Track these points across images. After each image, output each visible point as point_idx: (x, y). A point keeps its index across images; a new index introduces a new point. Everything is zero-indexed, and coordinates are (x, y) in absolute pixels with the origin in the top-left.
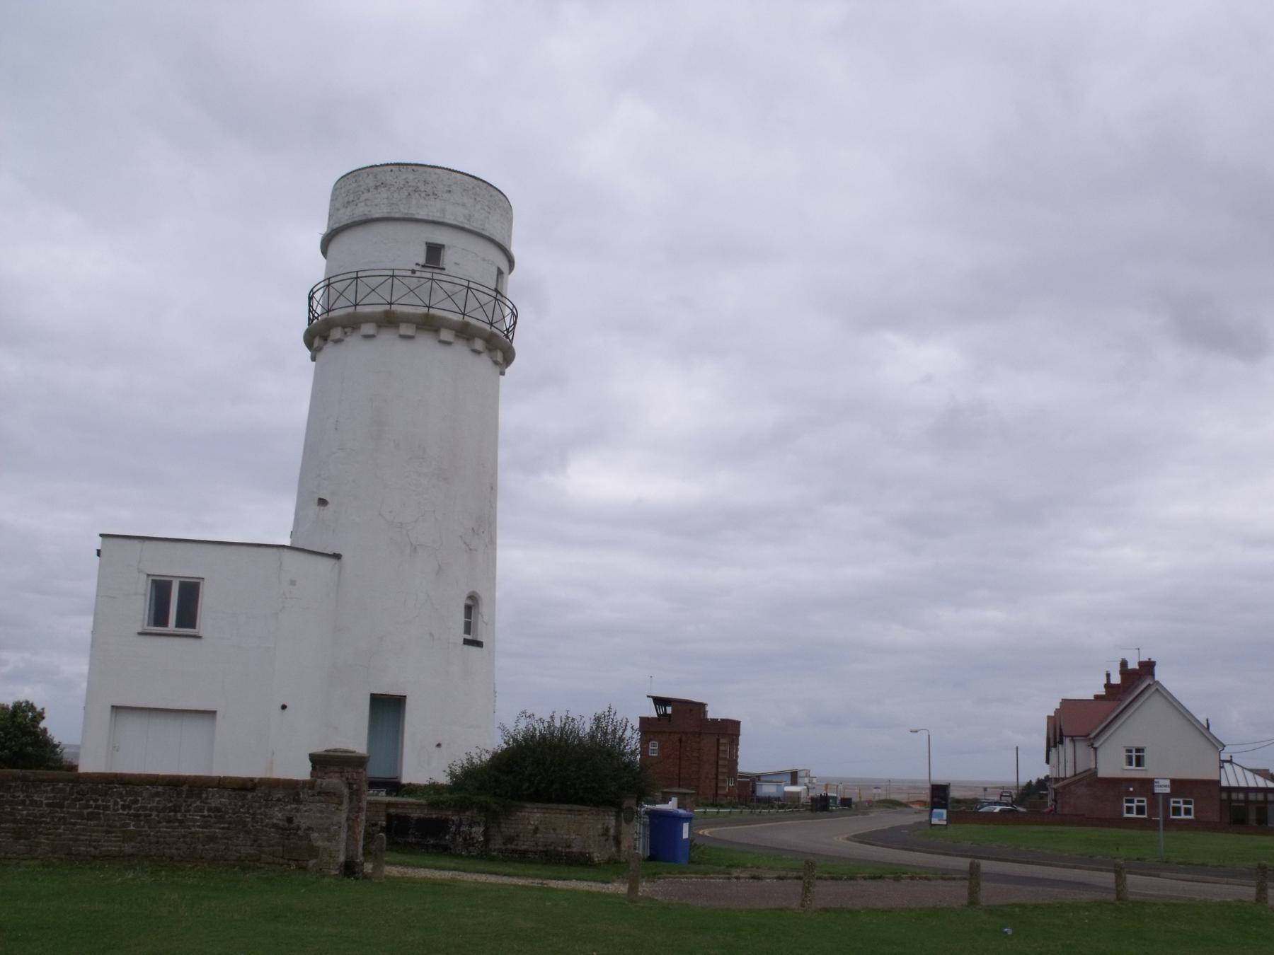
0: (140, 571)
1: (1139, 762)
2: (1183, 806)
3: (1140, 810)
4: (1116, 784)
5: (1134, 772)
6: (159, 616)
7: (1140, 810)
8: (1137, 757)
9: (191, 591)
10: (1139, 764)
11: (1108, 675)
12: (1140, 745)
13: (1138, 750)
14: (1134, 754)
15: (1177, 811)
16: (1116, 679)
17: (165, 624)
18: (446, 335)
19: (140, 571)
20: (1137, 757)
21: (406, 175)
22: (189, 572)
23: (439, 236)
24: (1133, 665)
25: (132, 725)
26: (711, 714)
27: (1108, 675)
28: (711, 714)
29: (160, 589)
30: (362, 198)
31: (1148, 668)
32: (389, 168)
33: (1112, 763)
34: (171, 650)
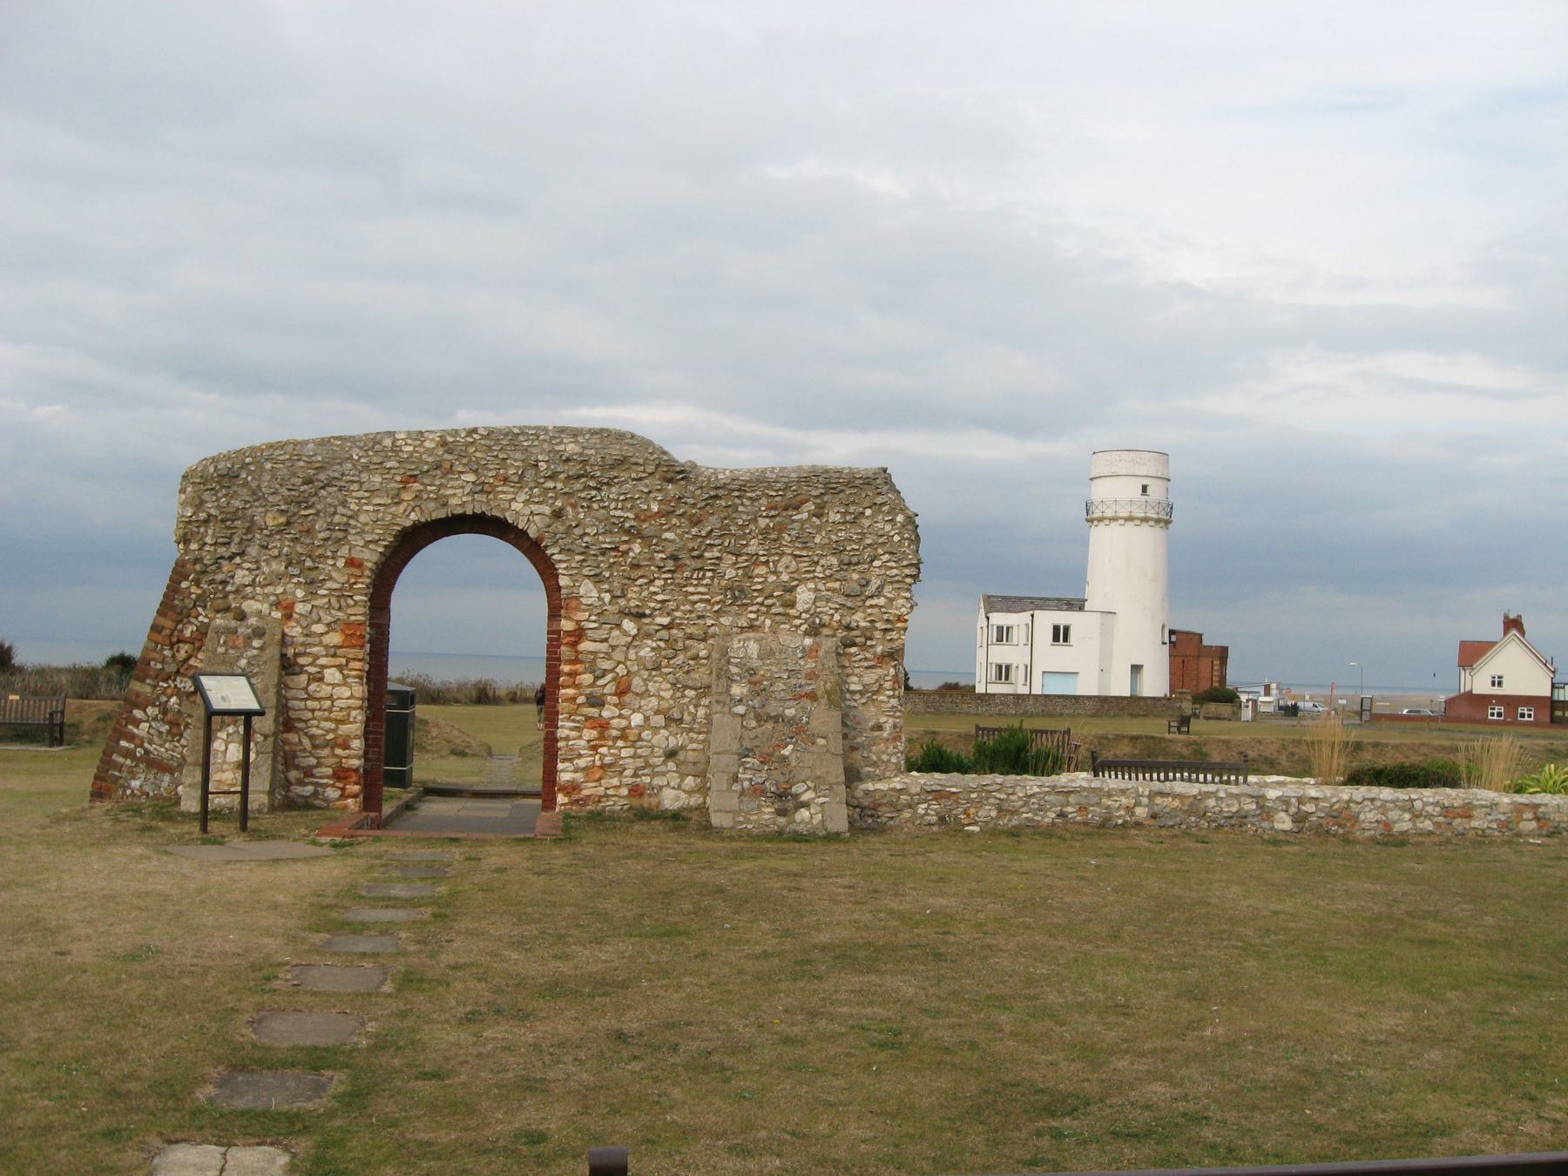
1: (1500, 684)
3: (1499, 715)
4: (1485, 700)
5: (1496, 691)
6: (1056, 638)
7: (1499, 715)
8: (1497, 682)
9: (1067, 629)
15: (1523, 715)
20: (1497, 682)
22: (1067, 623)
26: (1206, 642)
28: (1206, 642)
29: (1056, 629)
33: (1480, 683)
34: (1061, 649)
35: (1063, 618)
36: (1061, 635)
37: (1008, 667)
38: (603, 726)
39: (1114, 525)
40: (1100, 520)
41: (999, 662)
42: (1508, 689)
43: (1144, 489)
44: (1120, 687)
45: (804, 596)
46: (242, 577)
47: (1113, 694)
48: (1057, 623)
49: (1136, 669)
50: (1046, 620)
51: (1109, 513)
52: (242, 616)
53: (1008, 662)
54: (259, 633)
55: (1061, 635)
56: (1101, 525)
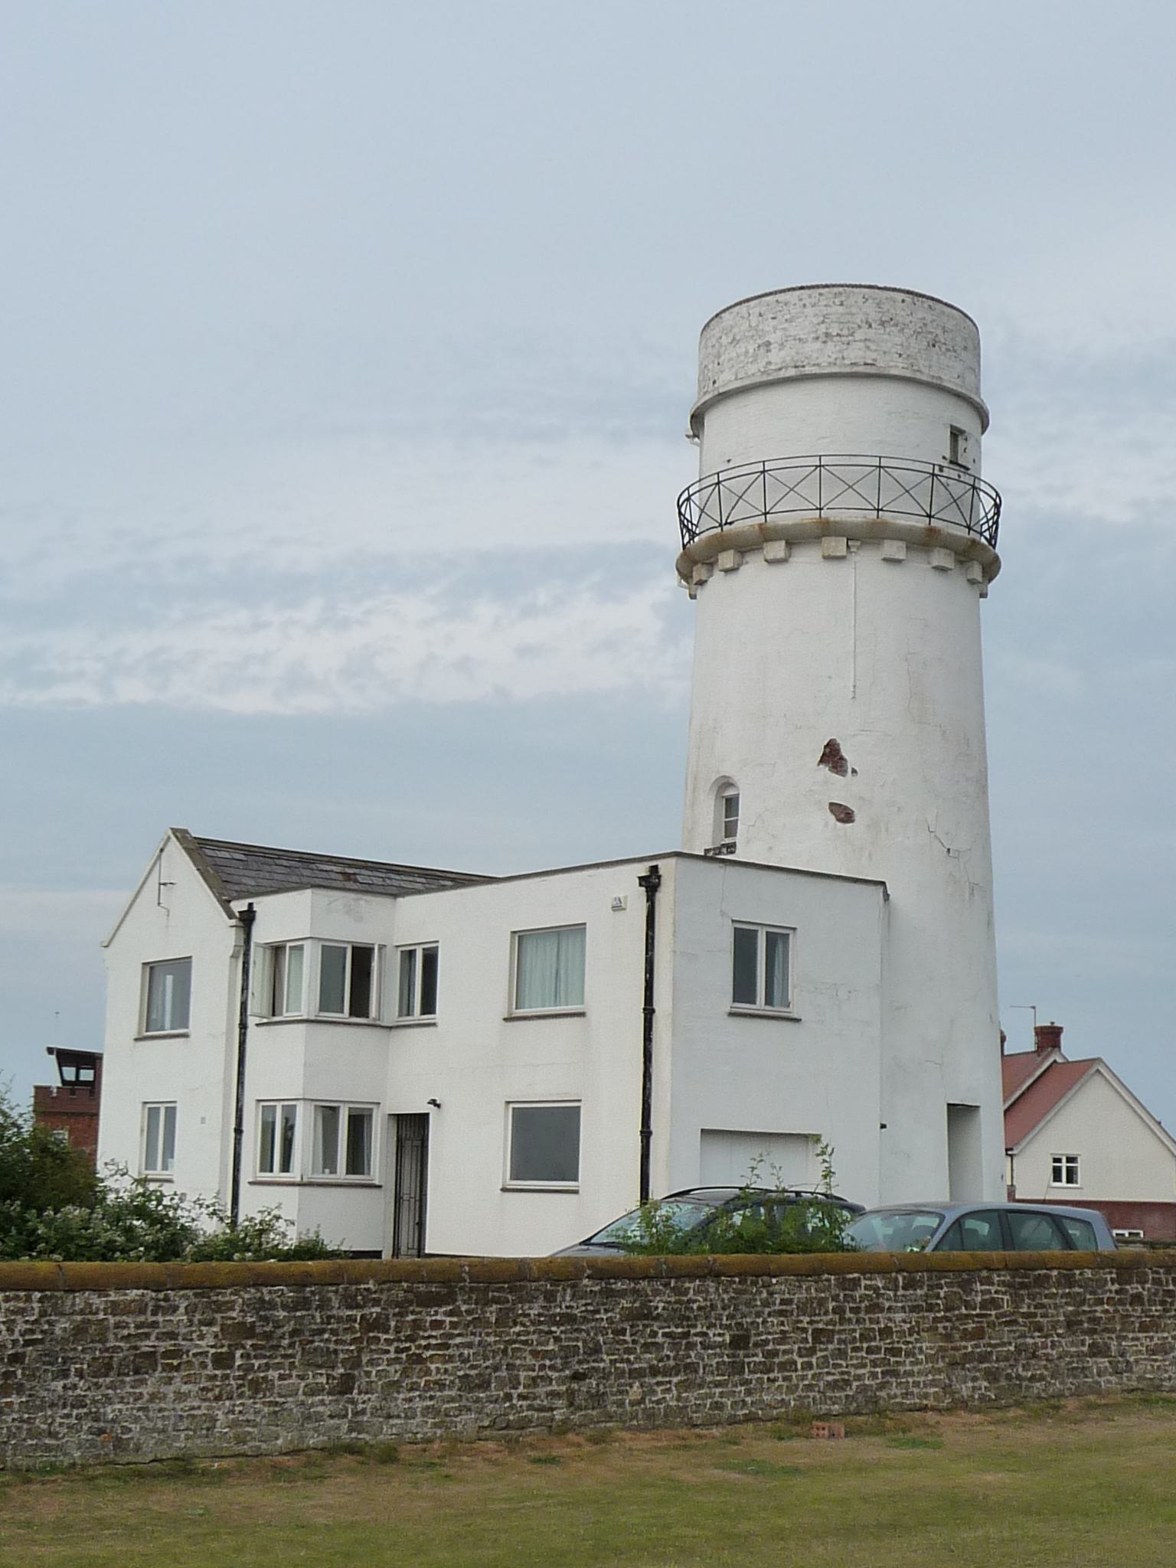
0: (723, 914)
5: (1063, 1191)
8: (1065, 1170)
10: (1071, 1179)
12: (1072, 1152)
13: (1070, 1160)
14: (1064, 1165)
17: (752, 1000)
19: (723, 914)
20: (1065, 1170)
21: (921, 312)
29: (744, 939)
30: (858, 336)
32: (900, 296)
39: (867, 564)
41: (329, 1093)
42: (1087, 1188)
51: (849, 510)
56: (807, 560)
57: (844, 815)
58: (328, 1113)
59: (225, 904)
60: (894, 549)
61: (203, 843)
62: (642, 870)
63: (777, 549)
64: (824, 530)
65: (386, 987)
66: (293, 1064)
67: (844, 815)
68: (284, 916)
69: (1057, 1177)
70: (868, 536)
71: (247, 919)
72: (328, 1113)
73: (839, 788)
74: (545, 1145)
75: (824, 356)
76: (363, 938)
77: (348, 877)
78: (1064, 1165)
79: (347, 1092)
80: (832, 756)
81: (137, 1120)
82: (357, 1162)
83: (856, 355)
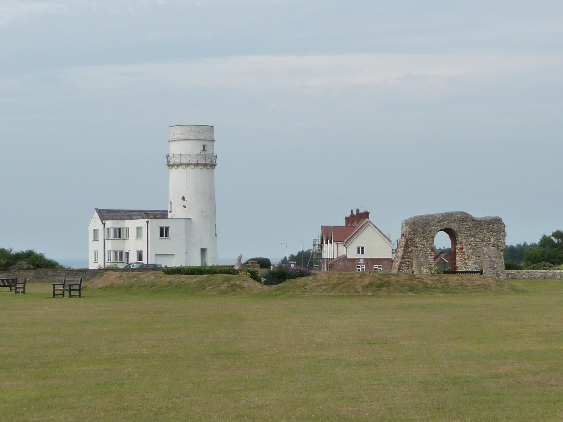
1: (363, 252)
2: (378, 268)
5: (360, 256)
6: (161, 235)
8: (361, 250)
9: (167, 229)
11: (352, 211)
12: (363, 246)
13: (362, 248)
14: (360, 249)
16: (355, 213)
18: (208, 167)
20: (361, 250)
21: (197, 128)
22: (167, 226)
23: (205, 143)
24: (361, 211)
25: (158, 258)
27: (352, 211)
29: (161, 229)
31: (366, 215)
33: (352, 253)
34: (164, 242)
35: (163, 223)
36: (164, 233)
37: (121, 253)
38: (466, 264)
39: (189, 168)
40: (173, 165)
41: (115, 250)
43: (204, 147)
44: (196, 262)
45: (492, 240)
46: (417, 240)
47: (90, 268)
48: (162, 225)
49: (203, 251)
50: (157, 224)
51: (185, 161)
52: (417, 247)
53: (121, 250)
54: (421, 250)
55: (164, 233)
56: (180, 168)
57: (185, 207)
58: (116, 253)
59: (102, 221)
60: (192, 166)
61: (100, 210)
62: (146, 220)
63: (176, 167)
64: (181, 164)
65: (124, 234)
66: (111, 245)
67: (185, 207)
68: (109, 224)
69: (358, 252)
70: (188, 165)
71: (104, 224)
72: (116, 253)
73: (184, 203)
74: (140, 257)
75: (182, 137)
76: (119, 227)
77: (125, 213)
78: (360, 249)
79: (118, 249)
80: (183, 199)
81: (93, 254)
82: (121, 259)
83: (186, 136)
